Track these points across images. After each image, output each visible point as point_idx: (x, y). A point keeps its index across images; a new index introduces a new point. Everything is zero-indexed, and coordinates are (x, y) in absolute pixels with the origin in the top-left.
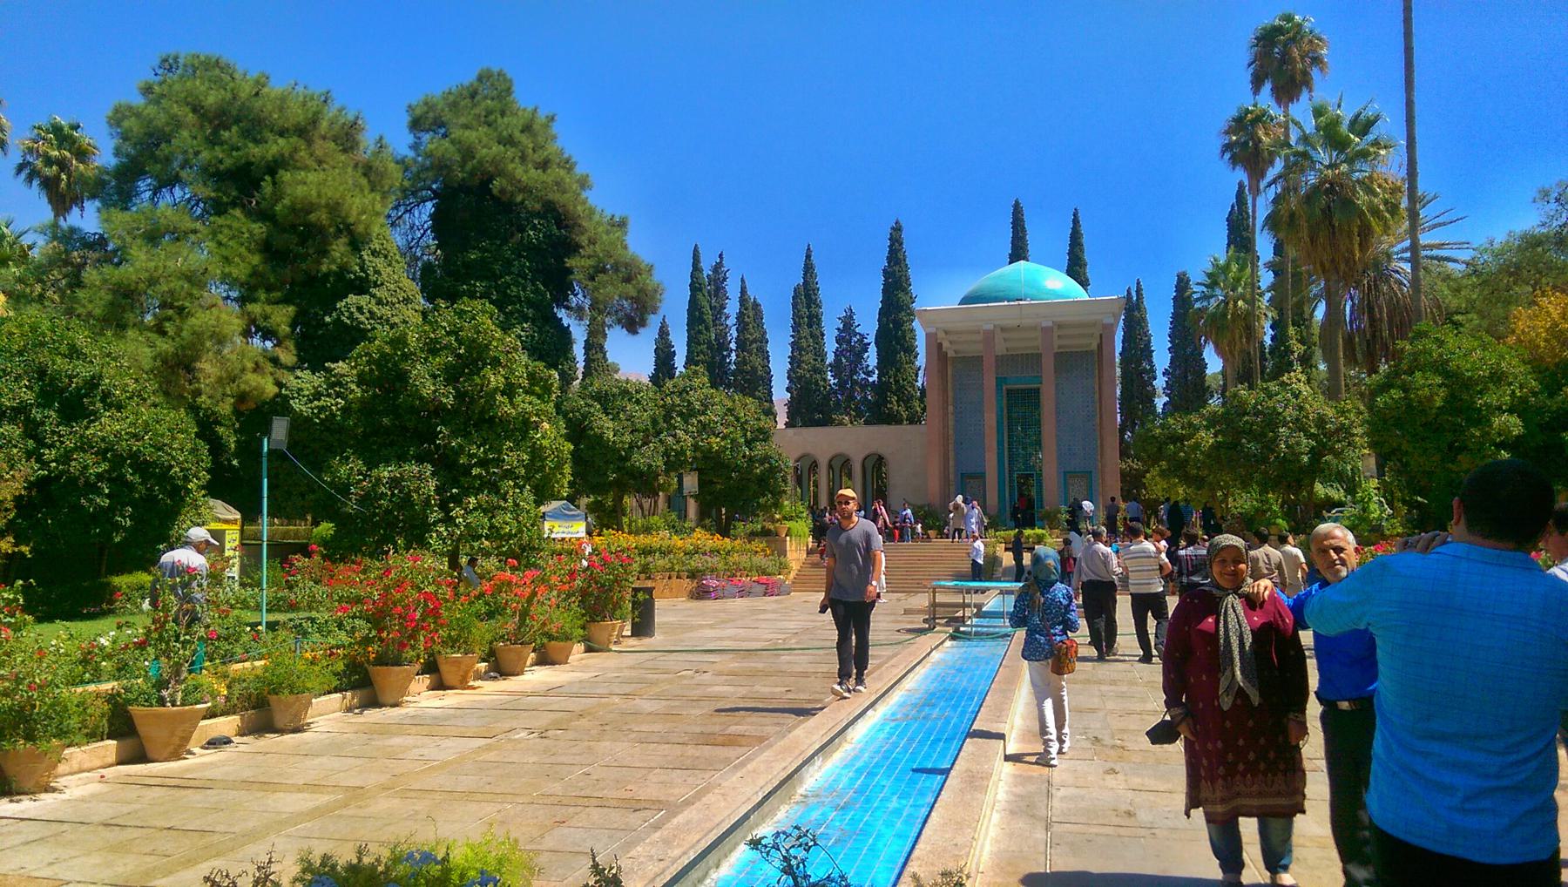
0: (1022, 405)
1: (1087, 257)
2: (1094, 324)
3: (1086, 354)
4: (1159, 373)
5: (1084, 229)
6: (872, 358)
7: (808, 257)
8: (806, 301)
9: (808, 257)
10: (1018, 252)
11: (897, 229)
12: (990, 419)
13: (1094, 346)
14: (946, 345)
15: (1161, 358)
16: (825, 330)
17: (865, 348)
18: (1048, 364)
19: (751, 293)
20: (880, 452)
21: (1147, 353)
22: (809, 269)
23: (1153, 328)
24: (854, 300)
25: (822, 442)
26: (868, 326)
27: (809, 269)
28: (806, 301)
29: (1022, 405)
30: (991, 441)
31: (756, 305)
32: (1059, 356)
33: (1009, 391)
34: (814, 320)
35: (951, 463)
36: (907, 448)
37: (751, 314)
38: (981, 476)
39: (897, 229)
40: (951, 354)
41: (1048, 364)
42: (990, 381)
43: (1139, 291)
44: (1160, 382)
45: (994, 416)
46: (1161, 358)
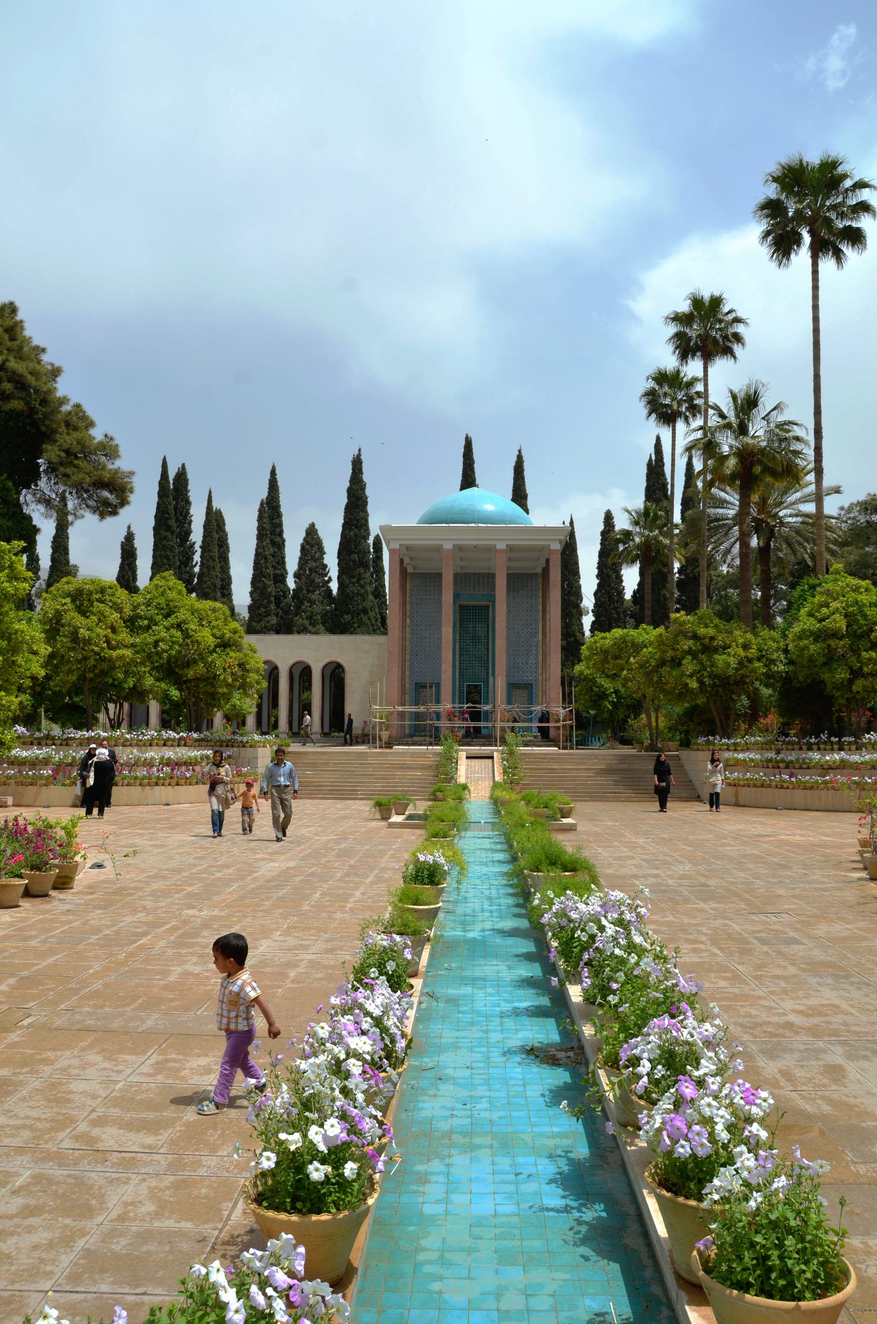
0: (474, 618)
2: (541, 549)
5: (526, 466)
7: (273, 473)
8: (270, 516)
12: (447, 632)
13: (539, 570)
14: (406, 560)
18: (501, 583)
19: (216, 505)
20: (339, 660)
24: (315, 512)
25: (282, 650)
28: (270, 516)
29: (474, 618)
30: (447, 655)
31: (219, 513)
32: (509, 576)
33: (462, 607)
35: (407, 673)
36: (362, 657)
37: (215, 523)
41: (501, 583)
42: (448, 596)
43: (572, 523)
45: (450, 630)
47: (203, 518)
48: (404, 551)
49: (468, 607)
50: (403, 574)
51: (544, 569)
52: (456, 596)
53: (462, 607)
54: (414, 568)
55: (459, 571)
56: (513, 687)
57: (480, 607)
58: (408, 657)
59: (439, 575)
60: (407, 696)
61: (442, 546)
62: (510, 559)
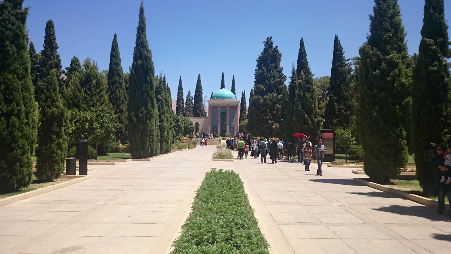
1: (235, 84)
3: (234, 107)
6: (193, 101)
7: (180, 79)
9: (180, 79)
10: (223, 86)
11: (199, 76)
16: (184, 94)
17: (192, 99)
21: (245, 103)
22: (180, 81)
23: (246, 99)
24: (189, 89)
26: (193, 95)
27: (180, 81)
29: (223, 115)
34: (182, 92)
39: (199, 76)
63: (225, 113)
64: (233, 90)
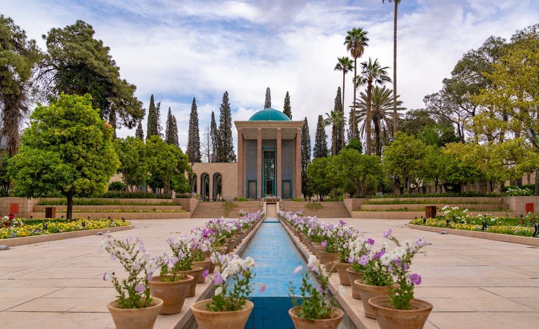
0: (269, 155)
4: (312, 149)
12: (260, 160)
13: (294, 139)
15: (313, 143)
18: (279, 143)
19: (172, 114)
20: (219, 172)
29: (269, 155)
30: (259, 168)
33: (265, 152)
35: (245, 177)
37: (171, 122)
38: (256, 181)
40: (245, 138)
41: (279, 143)
44: (312, 152)
45: (261, 159)
46: (313, 143)
47: (166, 119)
48: (243, 131)
49: (267, 152)
50: (243, 139)
51: (295, 138)
52: (263, 148)
53: (265, 152)
54: (247, 137)
55: (264, 139)
56: (283, 181)
57: (271, 152)
58: (245, 171)
59: (257, 140)
60: (245, 185)
61: (257, 129)
62: (282, 134)
63: (273, 154)
64: (287, 110)
